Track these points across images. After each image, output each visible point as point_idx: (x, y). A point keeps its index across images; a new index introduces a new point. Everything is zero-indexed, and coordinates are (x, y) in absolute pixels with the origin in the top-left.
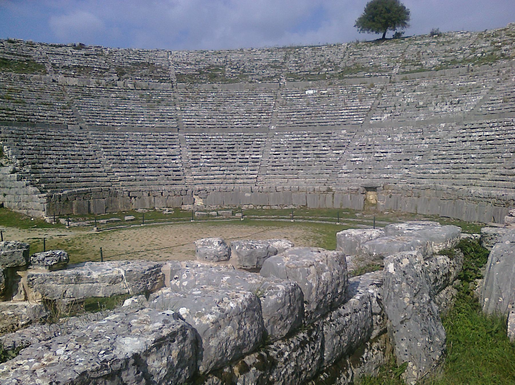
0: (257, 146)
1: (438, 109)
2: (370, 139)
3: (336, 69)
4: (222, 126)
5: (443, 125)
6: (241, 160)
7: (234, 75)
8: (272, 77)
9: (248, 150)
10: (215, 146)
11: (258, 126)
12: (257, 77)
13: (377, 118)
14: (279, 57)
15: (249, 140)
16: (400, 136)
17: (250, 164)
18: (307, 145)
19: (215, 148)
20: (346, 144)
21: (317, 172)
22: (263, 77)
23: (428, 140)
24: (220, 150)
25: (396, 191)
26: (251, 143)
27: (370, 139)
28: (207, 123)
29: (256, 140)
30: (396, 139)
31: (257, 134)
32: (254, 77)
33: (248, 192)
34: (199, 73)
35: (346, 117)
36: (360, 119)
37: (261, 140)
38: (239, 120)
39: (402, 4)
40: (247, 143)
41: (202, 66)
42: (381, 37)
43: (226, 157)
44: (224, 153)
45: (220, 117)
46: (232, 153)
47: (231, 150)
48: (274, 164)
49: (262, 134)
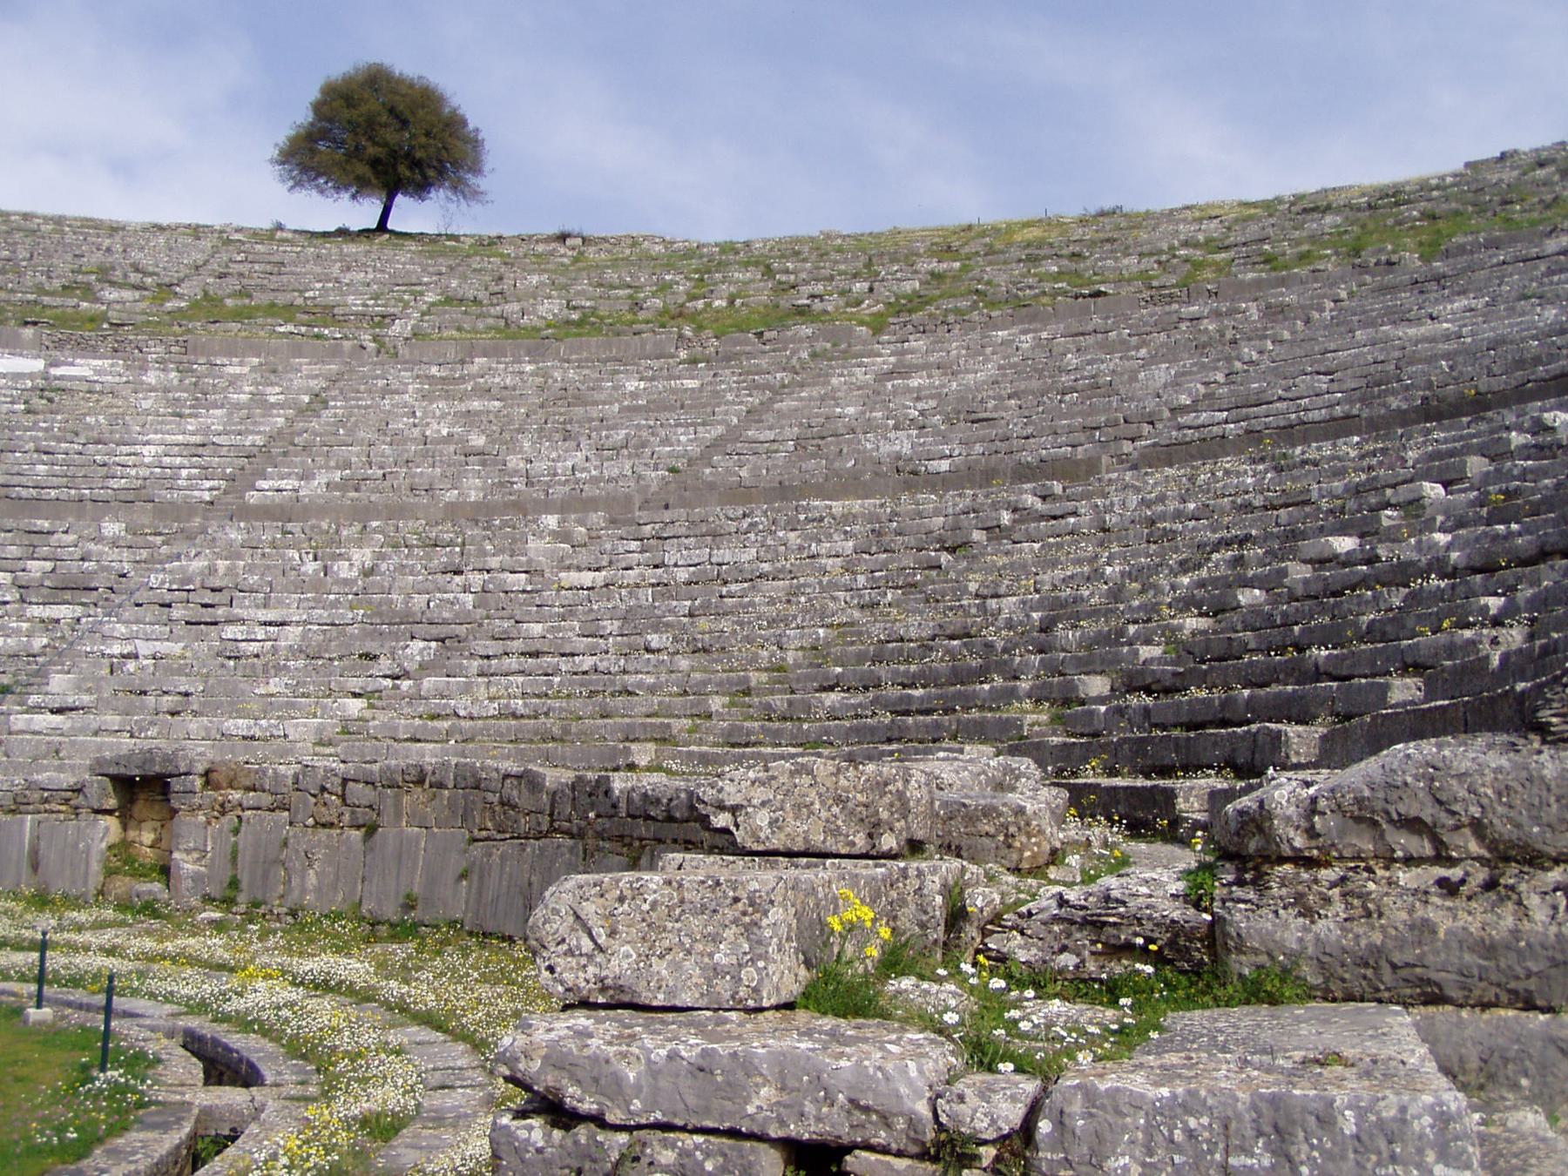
1: (541, 466)
2: (222, 565)
3: (159, 300)
5: (551, 521)
13: (283, 484)
23: (477, 579)
25: (266, 799)
27: (222, 565)
36: (208, 484)
39: (454, 111)
42: (374, 226)
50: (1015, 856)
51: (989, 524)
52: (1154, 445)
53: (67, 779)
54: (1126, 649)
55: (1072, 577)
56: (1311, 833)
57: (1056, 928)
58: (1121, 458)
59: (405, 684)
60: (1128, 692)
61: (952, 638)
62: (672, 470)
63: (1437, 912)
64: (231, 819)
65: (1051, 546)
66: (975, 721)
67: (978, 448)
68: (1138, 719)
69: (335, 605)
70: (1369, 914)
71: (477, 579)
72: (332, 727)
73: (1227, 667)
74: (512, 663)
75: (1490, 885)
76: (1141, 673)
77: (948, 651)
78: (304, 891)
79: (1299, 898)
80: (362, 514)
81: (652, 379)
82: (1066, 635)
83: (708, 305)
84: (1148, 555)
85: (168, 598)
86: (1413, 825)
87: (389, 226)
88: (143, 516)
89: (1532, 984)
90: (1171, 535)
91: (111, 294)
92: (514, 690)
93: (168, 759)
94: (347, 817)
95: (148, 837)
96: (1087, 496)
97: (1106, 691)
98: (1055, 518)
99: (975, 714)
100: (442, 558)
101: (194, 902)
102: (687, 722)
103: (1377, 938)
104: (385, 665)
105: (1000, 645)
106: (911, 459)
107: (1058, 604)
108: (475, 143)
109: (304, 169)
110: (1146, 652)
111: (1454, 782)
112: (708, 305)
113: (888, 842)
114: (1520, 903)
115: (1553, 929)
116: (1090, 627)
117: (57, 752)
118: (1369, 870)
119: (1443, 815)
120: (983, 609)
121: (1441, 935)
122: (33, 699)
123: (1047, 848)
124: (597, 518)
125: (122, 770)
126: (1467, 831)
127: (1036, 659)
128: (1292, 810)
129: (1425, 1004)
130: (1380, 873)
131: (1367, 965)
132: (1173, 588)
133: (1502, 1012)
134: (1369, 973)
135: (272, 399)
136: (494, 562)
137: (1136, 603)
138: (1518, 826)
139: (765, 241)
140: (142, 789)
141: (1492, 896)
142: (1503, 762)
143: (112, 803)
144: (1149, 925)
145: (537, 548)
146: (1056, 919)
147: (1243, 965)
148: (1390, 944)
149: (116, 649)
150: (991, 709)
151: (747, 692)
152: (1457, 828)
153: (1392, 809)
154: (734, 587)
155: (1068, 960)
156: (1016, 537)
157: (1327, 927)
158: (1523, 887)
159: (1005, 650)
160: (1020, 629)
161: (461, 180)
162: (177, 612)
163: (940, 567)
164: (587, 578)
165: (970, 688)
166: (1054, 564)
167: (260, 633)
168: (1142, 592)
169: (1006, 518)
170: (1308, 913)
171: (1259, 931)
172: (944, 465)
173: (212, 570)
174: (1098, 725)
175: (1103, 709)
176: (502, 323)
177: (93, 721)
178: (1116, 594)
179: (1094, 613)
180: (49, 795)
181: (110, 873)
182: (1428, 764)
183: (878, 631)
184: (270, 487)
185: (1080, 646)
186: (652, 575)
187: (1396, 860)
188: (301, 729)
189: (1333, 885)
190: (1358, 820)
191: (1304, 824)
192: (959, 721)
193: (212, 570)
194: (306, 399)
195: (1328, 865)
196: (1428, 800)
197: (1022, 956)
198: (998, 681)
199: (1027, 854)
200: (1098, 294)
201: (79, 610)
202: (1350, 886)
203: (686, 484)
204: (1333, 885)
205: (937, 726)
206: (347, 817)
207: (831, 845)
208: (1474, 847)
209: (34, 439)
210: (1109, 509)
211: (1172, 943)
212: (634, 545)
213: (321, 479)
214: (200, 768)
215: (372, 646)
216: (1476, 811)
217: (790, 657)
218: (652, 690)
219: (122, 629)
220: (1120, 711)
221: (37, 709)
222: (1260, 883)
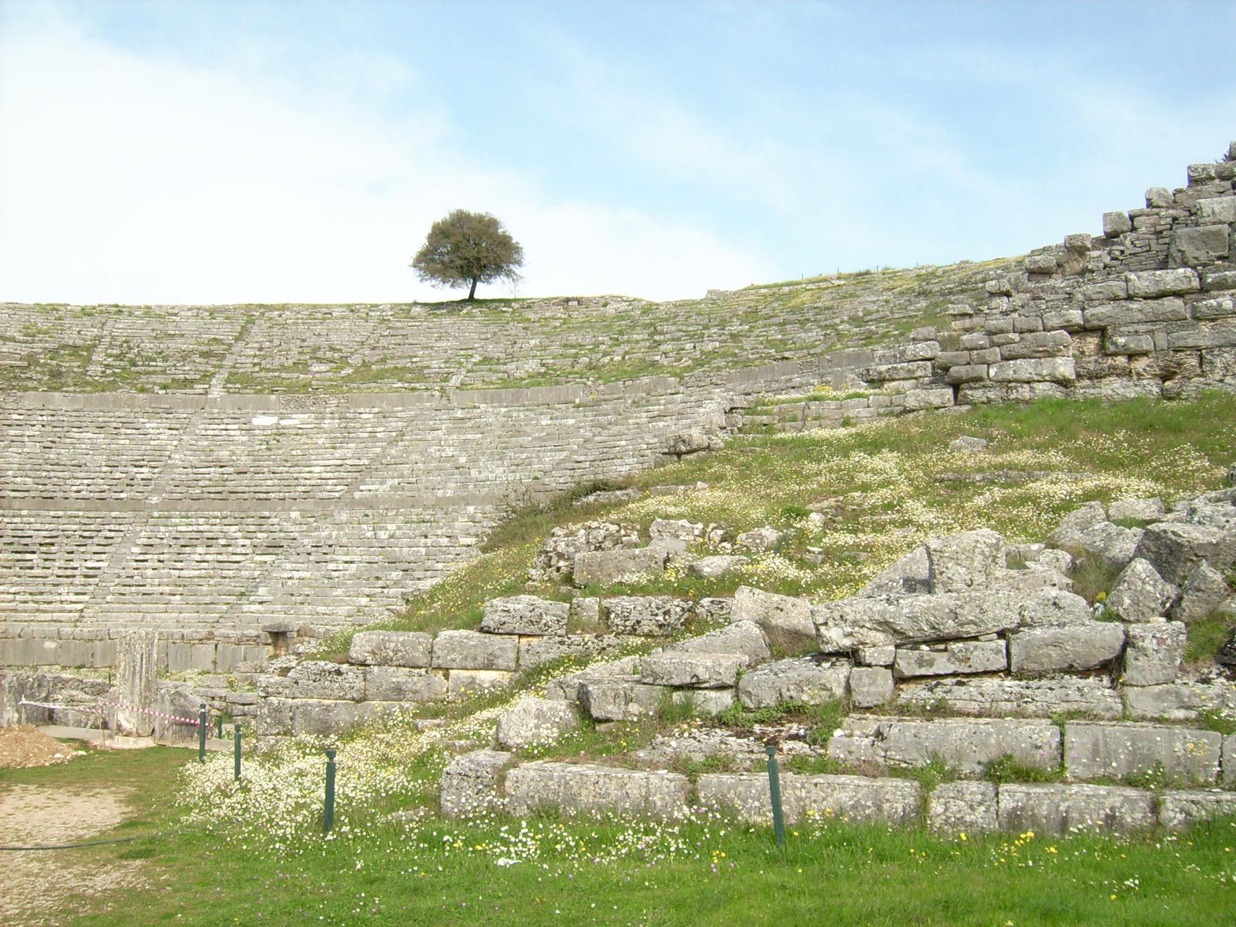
0: (105, 542)
4: (44, 494)
6: (60, 572)
7: (108, 372)
8: (192, 381)
9: (82, 549)
10: (12, 540)
11: (122, 495)
12: (160, 379)
13: (371, 487)
14: (226, 332)
15: (92, 527)
16: (392, 527)
18: (210, 542)
19: (12, 544)
20: (284, 543)
21: (208, 600)
22: (173, 380)
24: (21, 548)
26: (94, 534)
27: (334, 534)
28: (10, 487)
29: (107, 527)
30: (383, 535)
31: (113, 514)
32: (153, 378)
33: (51, 639)
34: (26, 364)
35: (313, 482)
36: (339, 488)
37: (117, 528)
38: (86, 482)
40: (86, 534)
41: (38, 347)
43: (29, 564)
44: (28, 556)
45: (44, 474)
46: (45, 556)
47: (44, 549)
48: (128, 581)
49: (124, 515)
53: (254, 633)
69: (374, 554)
81: (556, 418)
83: (612, 360)
87: (476, 296)
91: (315, 368)
108: (516, 249)
109: (426, 270)
112: (612, 360)
122: (252, 598)
139: (668, 303)
140: (278, 636)
143: (270, 641)
149: (286, 575)
161: (510, 271)
173: (330, 537)
176: (506, 376)
177: (272, 607)
188: (343, 610)
194: (394, 434)
200: (784, 358)
213: (390, 482)
215: (379, 574)
219: (289, 566)
221: (252, 603)
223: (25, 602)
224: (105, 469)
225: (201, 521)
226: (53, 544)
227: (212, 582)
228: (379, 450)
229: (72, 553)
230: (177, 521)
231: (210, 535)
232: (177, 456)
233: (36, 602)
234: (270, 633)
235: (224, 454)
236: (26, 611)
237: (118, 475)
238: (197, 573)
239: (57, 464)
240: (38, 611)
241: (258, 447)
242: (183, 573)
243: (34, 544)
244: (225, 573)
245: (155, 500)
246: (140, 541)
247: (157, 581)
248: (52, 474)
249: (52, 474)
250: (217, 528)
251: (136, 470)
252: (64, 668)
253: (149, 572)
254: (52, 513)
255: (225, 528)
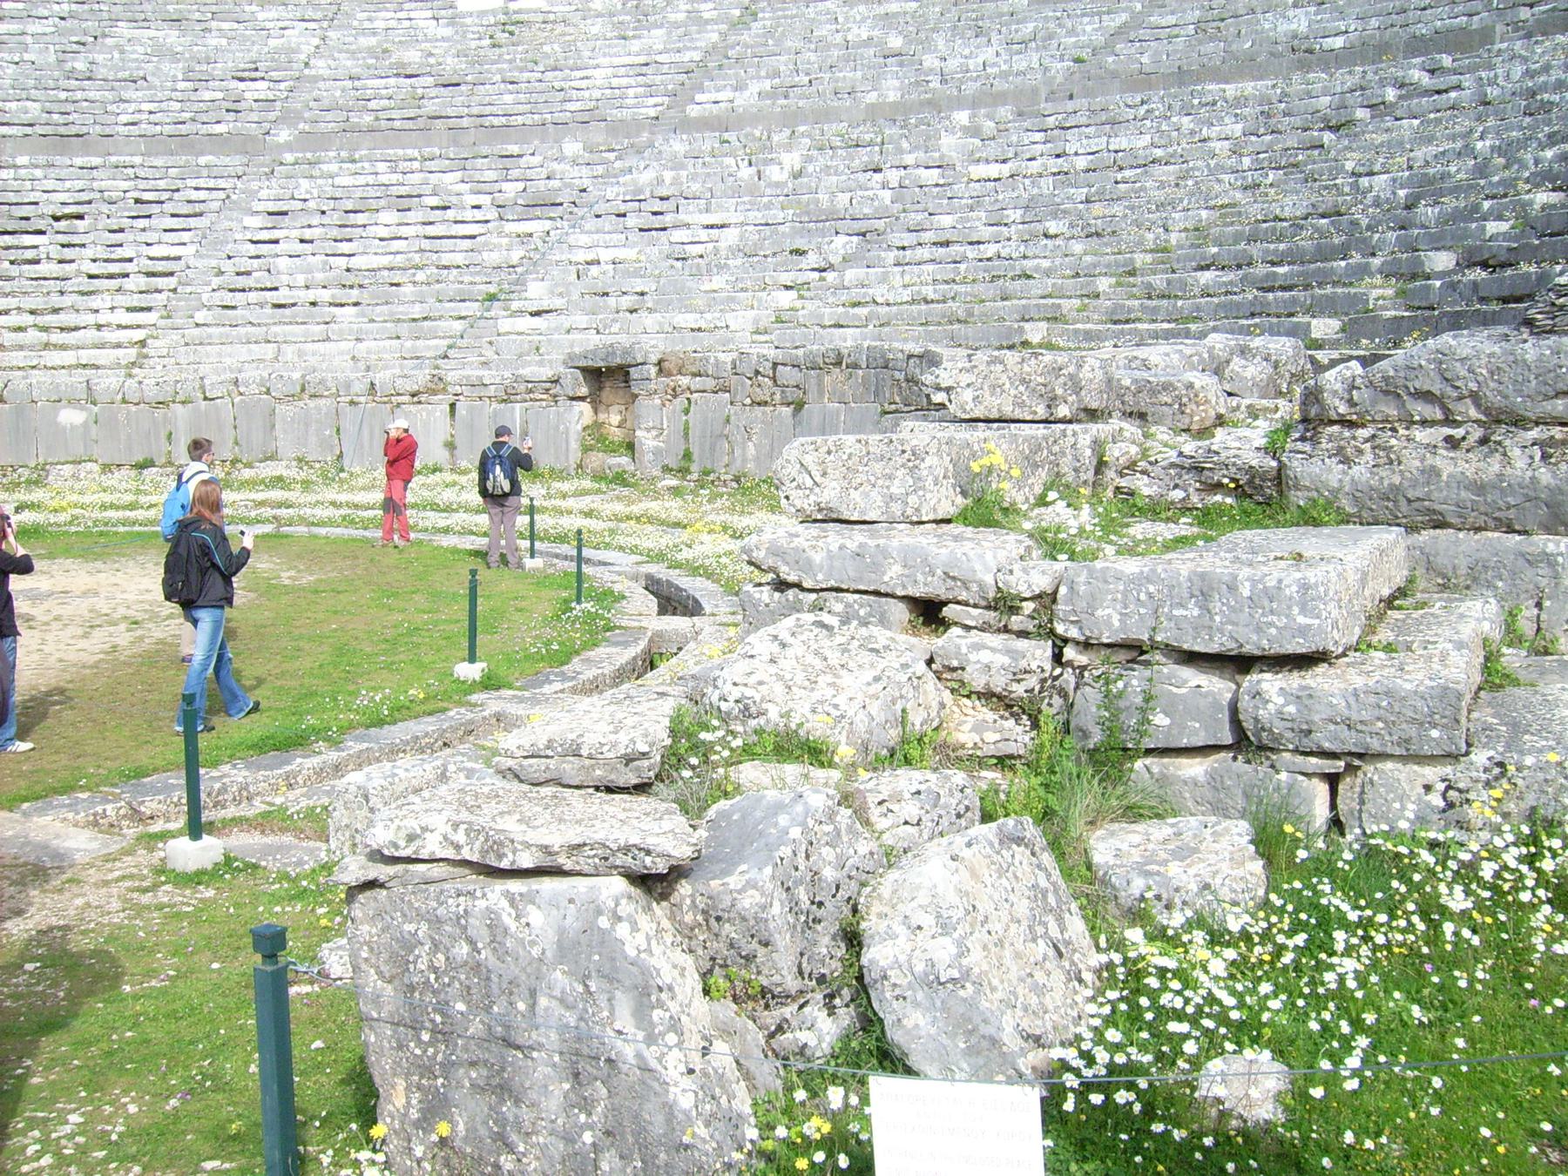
1: (953, 64)
2: (668, 176)
4: (62, 130)
5: (962, 117)
6: (95, 269)
11: (219, 129)
13: (720, 96)
15: (162, 184)
17: (136, 282)
18: (405, 203)
21: (417, 311)
23: (893, 176)
25: (710, 383)
27: (668, 176)
33: (73, 402)
36: (652, 101)
40: (147, 196)
43: (29, 254)
45: (63, 95)
48: (242, 282)
50: (1187, 421)
51: (1374, 101)
52: (1553, 10)
53: (546, 373)
54: (1474, 225)
55: (1443, 153)
56: (1351, 403)
57: (1172, 471)
58: (1516, 25)
59: (830, 276)
60: (1468, 267)
61: (1323, 216)
62: (1078, 61)
63: (1444, 462)
64: (680, 402)
65: (1429, 122)
66: (1326, 296)
67: (1374, 23)
68: (1468, 293)
69: (768, 206)
70: (1391, 463)
71: (893, 176)
72: (767, 318)
73: (1555, 243)
74: (924, 253)
75: (1484, 441)
76: (1480, 248)
77: (1317, 229)
78: (745, 460)
79: (1340, 450)
80: (790, 119)
82: (1427, 212)
84: (1522, 128)
85: (623, 208)
86: (1426, 396)
88: (598, 135)
89: (1512, 514)
90: (1547, 107)
92: (925, 278)
93: (626, 352)
94: (778, 397)
95: (615, 419)
96: (1471, 69)
97: (1452, 265)
98: (1438, 92)
99: (1329, 290)
100: (863, 157)
101: (656, 472)
102: (1076, 302)
103: (1397, 480)
104: (812, 259)
105: (1364, 222)
106: (1307, 38)
107: (1427, 181)
110: (1492, 227)
111: (1458, 364)
113: (1063, 411)
114: (1505, 454)
115: (1529, 473)
116: (1450, 203)
117: (537, 349)
118: (1394, 430)
119: (1449, 389)
120: (1355, 186)
121: (1444, 478)
122: (515, 305)
123: (1212, 413)
124: (1005, 112)
125: (590, 363)
126: (1468, 401)
127: (1392, 236)
128: (1338, 386)
129: (1435, 527)
130: (1402, 432)
131: (1388, 499)
132: (1536, 163)
133: (1490, 534)
134: (1390, 504)
135: (706, 15)
136: (909, 159)
137: (1496, 179)
138: (1506, 397)
140: (607, 378)
141: (1485, 449)
142: (1496, 349)
143: (584, 391)
144: (1234, 470)
145: (950, 144)
146: (1173, 465)
147: (1298, 498)
148: (1406, 484)
149: (581, 256)
150: (1345, 285)
151: (1132, 273)
152: (1460, 399)
153: (1410, 385)
154: (1128, 173)
155: (1178, 495)
156: (1399, 113)
157: (1360, 471)
158: (1507, 443)
159: (1369, 228)
160: (1386, 207)
162: (631, 221)
163: (1322, 146)
164: (994, 170)
165: (1328, 265)
166: (1430, 140)
167: (703, 235)
168: (1506, 167)
169: (1391, 94)
170: (1346, 461)
171: (1310, 475)
172: (1338, 42)
173: (660, 181)
174: (1434, 299)
175: (1438, 283)
177: (565, 321)
178: (1482, 170)
179: (1456, 190)
180: (532, 385)
181: (586, 449)
182: (1438, 351)
183: (1255, 211)
184: (710, 99)
185: (1438, 223)
186: (1054, 165)
187: (1414, 423)
188: (741, 321)
189: (1367, 441)
190: (1387, 393)
191: (1346, 396)
192: (1312, 297)
193: (660, 181)
194: (737, 12)
195: (1363, 426)
196: (1438, 379)
197: (1146, 491)
198: (1356, 258)
199: (1196, 418)
201: (548, 225)
202: (1378, 441)
203: (1089, 74)
204: (1367, 441)
205: (1294, 300)
206: (778, 397)
207: (1018, 414)
208: (1473, 413)
209: (500, 71)
210: (1492, 82)
211: (1250, 482)
212: (1039, 136)
213: (754, 88)
214: (654, 358)
215: (800, 244)
216: (1473, 386)
217: (1174, 238)
218: (1048, 273)
219: (584, 239)
220: (1453, 286)
222: (1314, 441)
223: (20, 329)
224: (182, 85)
225: (382, 167)
226: (80, 217)
227: (421, 276)
228: (715, 37)
229: (121, 230)
230: (334, 167)
231: (403, 191)
232: (321, 63)
233: (45, 329)
234: (584, 370)
235: (413, 56)
236: (21, 348)
237: (207, 95)
238: (385, 261)
239: (89, 79)
240: (47, 346)
241: (474, 44)
242: (354, 262)
243: (42, 216)
244: (446, 259)
245: (283, 135)
246: (260, 207)
247: (301, 280)
248: (79, 95)
249: (79, 95)
250: (416, 178)
251: (242, 85)
252: (106, 468)
253: (283, 263)
254: (79, 161)
255: (434, 178)
